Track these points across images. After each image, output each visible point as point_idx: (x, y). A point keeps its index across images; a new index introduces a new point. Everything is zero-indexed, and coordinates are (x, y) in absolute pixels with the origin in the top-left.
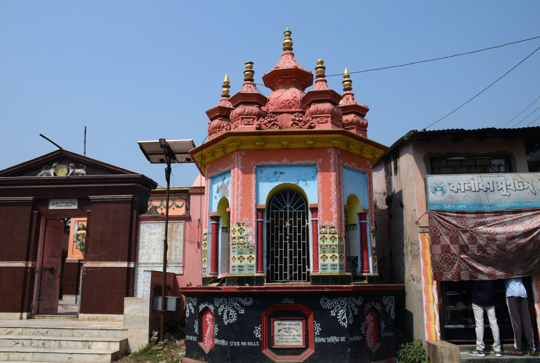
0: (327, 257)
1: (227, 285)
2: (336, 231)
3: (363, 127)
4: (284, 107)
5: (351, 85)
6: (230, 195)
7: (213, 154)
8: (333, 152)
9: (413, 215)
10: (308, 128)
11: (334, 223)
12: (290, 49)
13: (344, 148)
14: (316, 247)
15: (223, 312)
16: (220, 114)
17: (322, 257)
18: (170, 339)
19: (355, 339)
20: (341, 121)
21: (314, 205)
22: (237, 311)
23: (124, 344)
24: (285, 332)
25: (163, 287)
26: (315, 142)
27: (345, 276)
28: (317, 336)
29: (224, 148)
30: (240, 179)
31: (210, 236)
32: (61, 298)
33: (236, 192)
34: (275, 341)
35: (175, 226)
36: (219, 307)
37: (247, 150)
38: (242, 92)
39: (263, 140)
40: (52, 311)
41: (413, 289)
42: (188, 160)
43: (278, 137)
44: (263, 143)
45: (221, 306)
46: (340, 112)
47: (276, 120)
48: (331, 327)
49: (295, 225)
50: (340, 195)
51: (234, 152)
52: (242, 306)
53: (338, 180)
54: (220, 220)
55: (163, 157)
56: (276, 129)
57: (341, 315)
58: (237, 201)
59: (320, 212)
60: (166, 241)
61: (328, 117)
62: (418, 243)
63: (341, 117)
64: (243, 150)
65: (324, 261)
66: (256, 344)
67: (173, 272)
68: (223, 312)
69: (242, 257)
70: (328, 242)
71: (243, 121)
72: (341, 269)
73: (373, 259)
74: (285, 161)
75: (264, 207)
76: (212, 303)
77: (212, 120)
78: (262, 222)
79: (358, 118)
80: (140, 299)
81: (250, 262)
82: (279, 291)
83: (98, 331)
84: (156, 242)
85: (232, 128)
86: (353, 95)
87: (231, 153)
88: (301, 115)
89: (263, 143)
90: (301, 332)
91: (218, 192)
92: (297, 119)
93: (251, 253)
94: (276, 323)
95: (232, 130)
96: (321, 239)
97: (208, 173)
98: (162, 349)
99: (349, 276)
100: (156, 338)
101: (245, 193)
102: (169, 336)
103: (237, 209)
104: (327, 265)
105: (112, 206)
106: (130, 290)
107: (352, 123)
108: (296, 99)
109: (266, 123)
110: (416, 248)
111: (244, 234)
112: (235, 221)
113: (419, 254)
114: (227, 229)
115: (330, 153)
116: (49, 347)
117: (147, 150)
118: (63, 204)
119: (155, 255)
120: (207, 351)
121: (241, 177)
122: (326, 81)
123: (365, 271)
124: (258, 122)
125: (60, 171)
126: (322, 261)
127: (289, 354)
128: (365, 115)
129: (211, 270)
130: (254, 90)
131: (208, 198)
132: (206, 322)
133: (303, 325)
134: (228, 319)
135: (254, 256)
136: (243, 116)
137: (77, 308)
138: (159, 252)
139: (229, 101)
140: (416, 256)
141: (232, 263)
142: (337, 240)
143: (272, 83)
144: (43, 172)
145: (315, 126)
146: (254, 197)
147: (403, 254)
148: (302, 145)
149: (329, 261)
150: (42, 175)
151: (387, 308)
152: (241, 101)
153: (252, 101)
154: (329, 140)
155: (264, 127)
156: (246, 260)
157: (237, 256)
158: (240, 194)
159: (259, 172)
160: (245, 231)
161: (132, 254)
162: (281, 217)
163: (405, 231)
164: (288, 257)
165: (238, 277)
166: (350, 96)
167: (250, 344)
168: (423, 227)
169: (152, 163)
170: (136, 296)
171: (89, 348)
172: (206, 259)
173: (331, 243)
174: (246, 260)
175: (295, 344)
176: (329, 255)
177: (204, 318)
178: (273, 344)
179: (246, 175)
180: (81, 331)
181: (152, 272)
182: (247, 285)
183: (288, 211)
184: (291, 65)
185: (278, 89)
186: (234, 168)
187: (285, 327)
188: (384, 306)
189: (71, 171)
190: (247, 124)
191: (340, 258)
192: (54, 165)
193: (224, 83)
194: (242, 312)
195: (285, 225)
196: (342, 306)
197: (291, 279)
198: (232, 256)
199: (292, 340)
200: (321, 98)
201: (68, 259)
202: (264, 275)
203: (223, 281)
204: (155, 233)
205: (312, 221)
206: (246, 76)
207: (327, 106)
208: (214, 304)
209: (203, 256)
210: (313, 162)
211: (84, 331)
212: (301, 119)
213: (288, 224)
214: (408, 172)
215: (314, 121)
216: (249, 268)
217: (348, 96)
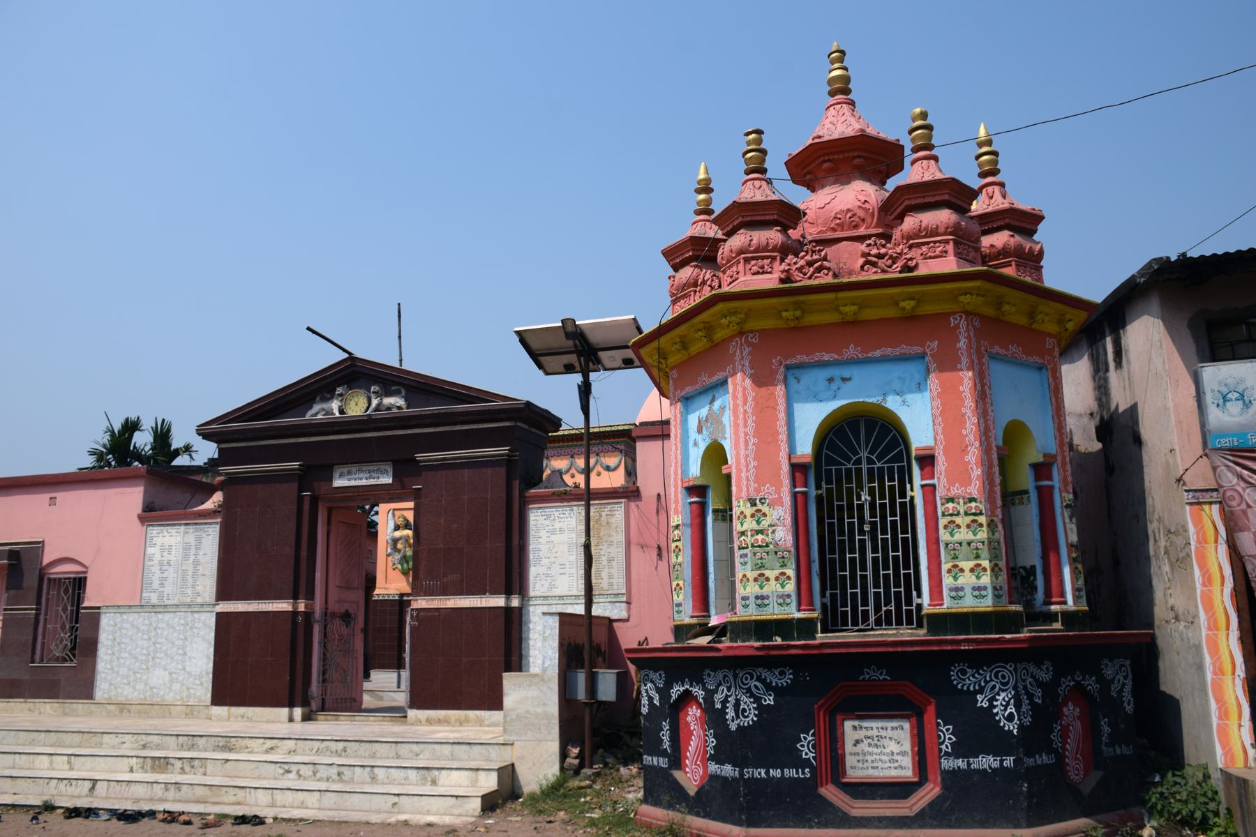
0: (962, 570)
1: (732, 640)
3: (1033, 260)
4: (841, 226)
5: (996, 162)
6: (727, 435)
7: (684, 345)
8: (963, 324)
9: (1168, 464)
10: (900, 272)
11: (975, 489)
12: (846, 91)
13: (989, 311)
14: (935, 547)
15: (725, 702)
16: (696, 252)
17: (949, 571)
18: (606, 765)
19: (1039, 762)
20: (978, 249)
21: (924, 449)
22: (757, 700)
23: (508, 774)
24: (870, 745)
25: (587, 647)
26: (919, 301)
27: (1008, 612)
28: (947, 754)
29: (709, 329)
30: (750, 399)
31: (688, 532)
32: (367, 676)
33: (742, 430)
34: (848, 768)
36: (716, 691)
37: (762, 332)
38: (743, 200)
39: (797, 306)
40: (350, 704)
41: (1178, 641)
42: (628, 363)
43: (831, 296)
44: (798, 313)
45: (720, 689)
46: (976, 228)
47: (825, 259)
48: (978, 732)
49: (882, 497)
50: (986, 421)
51: (732, 337)
52: (768, 687)
53: (979, 387)
54: (710, 494)
55: (572, 358)
56: (827, 279)
57: (1003, 706)
58: (746, 449)
59: (941, 465)
60: (587, 547)
61: (947, 242)
62: (1186, 531)
63: (978, 241)
64: (752, 331)
65: (956, 578)
66: (803, 773)
67: (607, 614)
68: (725, 702)
69: (762, 575)
70: (963, 535)
71: (749, 266)
72: (997, 597)
73: (1074, 571)
74: (852, 351)
75: (809, 460)
76: (699, 681)
77: (676, 268)
78: (805, 494)
79: (1018, 239)
80: (536, 675)
81: (783, 587)
83: (449, 747)
84: (566, 548)
85: (724, 284)
86: (1002, 185)
87: (726, 341)
88: (883, 242)
89: (798, 313)
90: (907, 746)
91: (700, 431)
92: (874, 251)
93: (784, 566)
94: (848, 725)
95: (725, 289)
96: (946, 527)
97: (676, 389)
98: (590, 787)
99: (1016, 612)
100: (576, 762)
101: (764, 434)
102: (603, 757)
103: (747, 466)
104: (962, 589)
105: (466, 472)
106: (513, 658)
107: (1004, 252)
108: (867, 206)
109: (802, 267)
110: (1179, 541)
111: (765, 523)
112: (744, 494)
113: (1188, 555)
114: (725, 515)
115: (957, 326)
116: (352, 781)
117: (535, 345)
118: (361, 475)
120: (692, 791)
122: (936, 159)
123: (1054, 600)
124: (784, 266)
125: (352, 403)
126: (951, 579)
127: (882, 797)
128: (1035, 232)
129: (694, 607)
130: (769, 193)
131: (679, 445)
132: (688, 724)
133: (912, 730)
134: (738, 717)
135: (791, 572)
136: (748, 255)
137: (401, 698)
138: (574, 571)
139: (715, 221)
140: (1181, 562)
141: (741, 591)
142: (985, 528)
143: (808, 173)
144: (316, 408)
145: (917, 265)
146: (783, 437)
147: (1148, 558)
148: (890, 313)
149: (967, 580)
150: (316, 414)
151: (1114, 688)
153: (767, 218)
155: (797, 276)
156: (773, 582)
157: (751, 575)
158: (751, 433)
159: (792, 380)
160: (768, 517)
161: (513, 575)
162: (849, 481)
163: (1149, 501)
164: (869, 573)
165: (755, 621)
166: (997, 188)
167: (790, 773)
168: (1196, 491)
169: (547, 374)
170: (528, 671)
171: (434, 782)
172: (681, 583)
173: (970, 536)
174: (773, 582)
175: (894, 773)
176: (967, 565)
177: (681, 715)
178: (844, 773)
179: (764, 389)
180: (414, 747)
181: (562, 615)
182: (778, 640)
183: (864, 466)
184: (850, 129)
185: (823, 187)
186: (734, 374)
187: (869, 733)
188: (1105, 684)
189: (375, 402)
190: (758, 273)
191: (993, 570)
192: (339, 390)
193: (699, 182)
195: (859, 498)
196: (1003, 684)
197: (878, 622)
198: (739, 575)
199: (888, 764)
200: (928, 200)
201: (376, 592)
202: (815, 615)
203: (721, 631)
204: (561, 530)
205: (923, 486)
206: (747, 162)
207: (944, 216)
208: (704, 685)
209: (674, 576)
210: (917, 349)
211: (422, 746)
212: (883, 251)
213: (865, 497)
214: (1150, 359)
215: (915, 253)
216: (781, 601)
217: (990, 189)
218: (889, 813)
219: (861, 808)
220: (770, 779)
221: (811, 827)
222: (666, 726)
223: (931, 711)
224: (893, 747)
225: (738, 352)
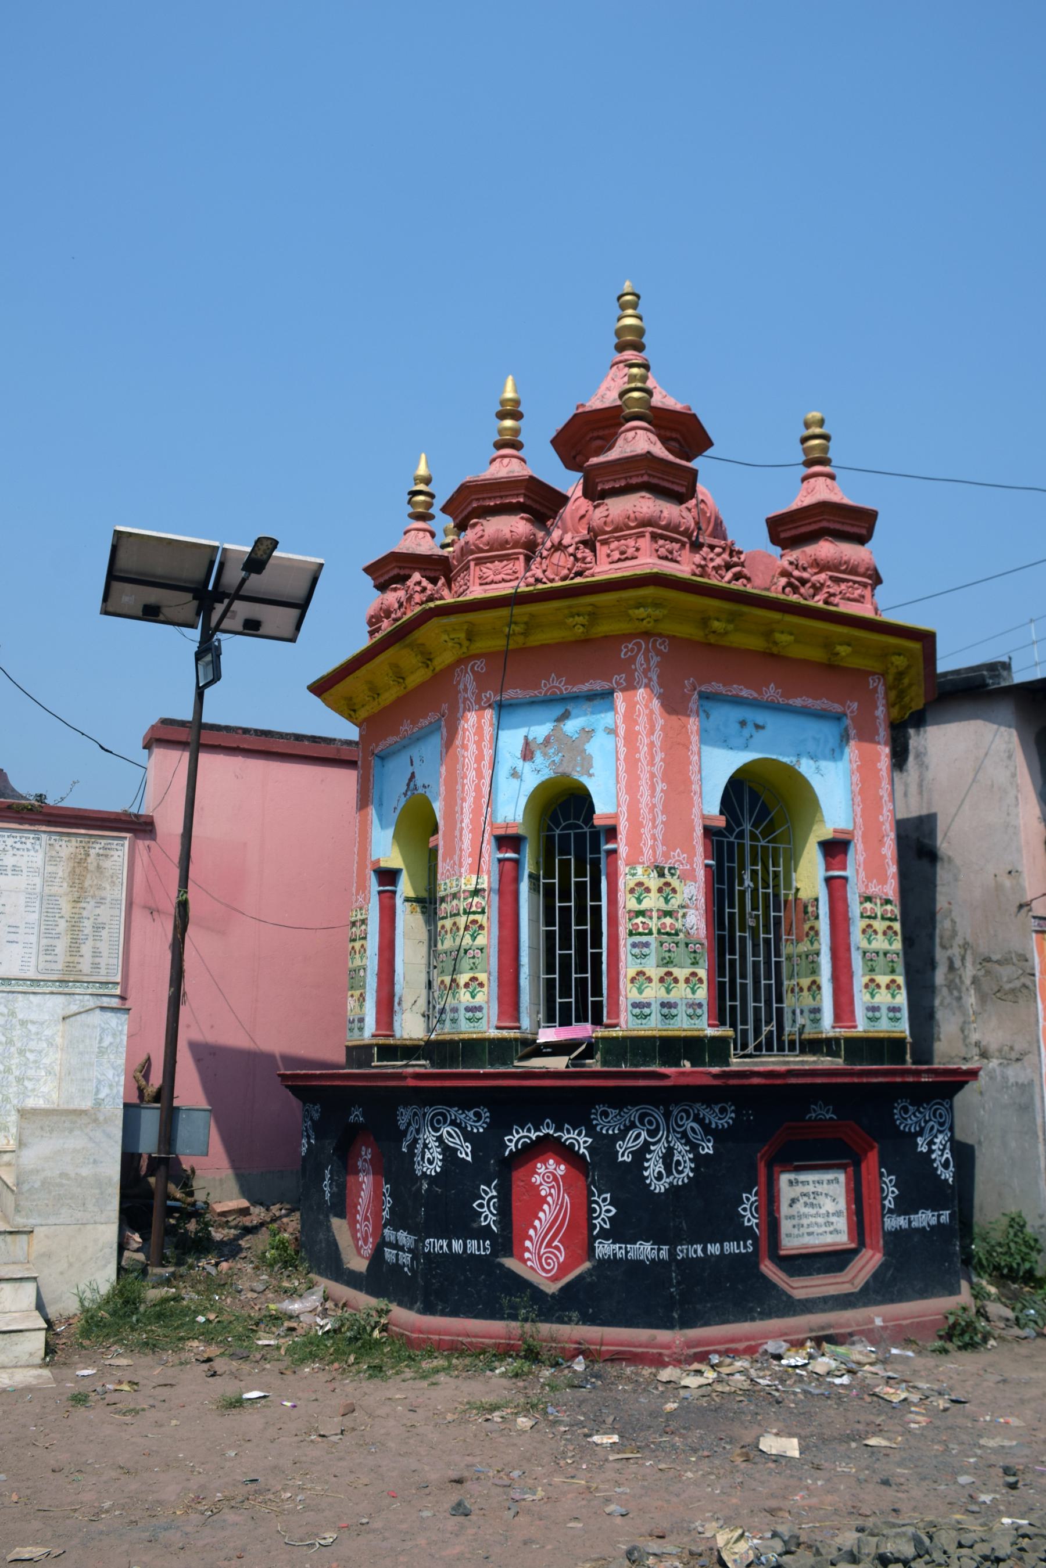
2: (897, 912)
8: (881, 689)
21: (843, 832)
22: (694, 1147)
24: (806, 1204)
28: (890, 1211)
30: (658, 728)
31: (495, 898)
34: (783, 1236)
35: (96, 848)
37: (672, 638)
39: (732, 618)
43: (776, 616)
52: (707, 1129)
58: (653, 796)
59: (856, 856)
64: (660, 635)
66: (745, 1247)
70: (880, 943)
74: (771, 692)
76: (581, 1121)
81: (694, 992)
82: (819, 1080)
84: (22, 899)
90: (842, 1205)
93: (695, 963)
94: (784, 1178)
100: (141, 1257)
103: (654, 820)
111: (675, 903)
115: (876, 688)
119: (17, 949)
121: (660, 722)
126: (867, 997)
127: (819, 1271)
132: (536, 1188)
133: (847, 1184)
138: (33, 939)
152: (645, 478)
153: (676, 488)
154: (884, 654)
156: (682, 984)
157: (654, 972)
163: (943, 925)
172: (482, 977)
174: (682, 984)
176: (883, 980)
179: (674, 718)
183: (747, 842)
186: (630, 686)
190: (666, 558)
194: (708, 1148)
195: (741, 883)
196: (942, 1124)
197: (758, 1048)
199: (824, 1229)
210: (837, 708)
212: (805, 575)
216: (690, 1011)
218: (832, 1291)
219: (802, 1288)
220: (708, 1258)
221: (753, 1319)
222: (489, 1192)
223: (873, 1158)
224: (828, 1206)
225: (640, 658)
